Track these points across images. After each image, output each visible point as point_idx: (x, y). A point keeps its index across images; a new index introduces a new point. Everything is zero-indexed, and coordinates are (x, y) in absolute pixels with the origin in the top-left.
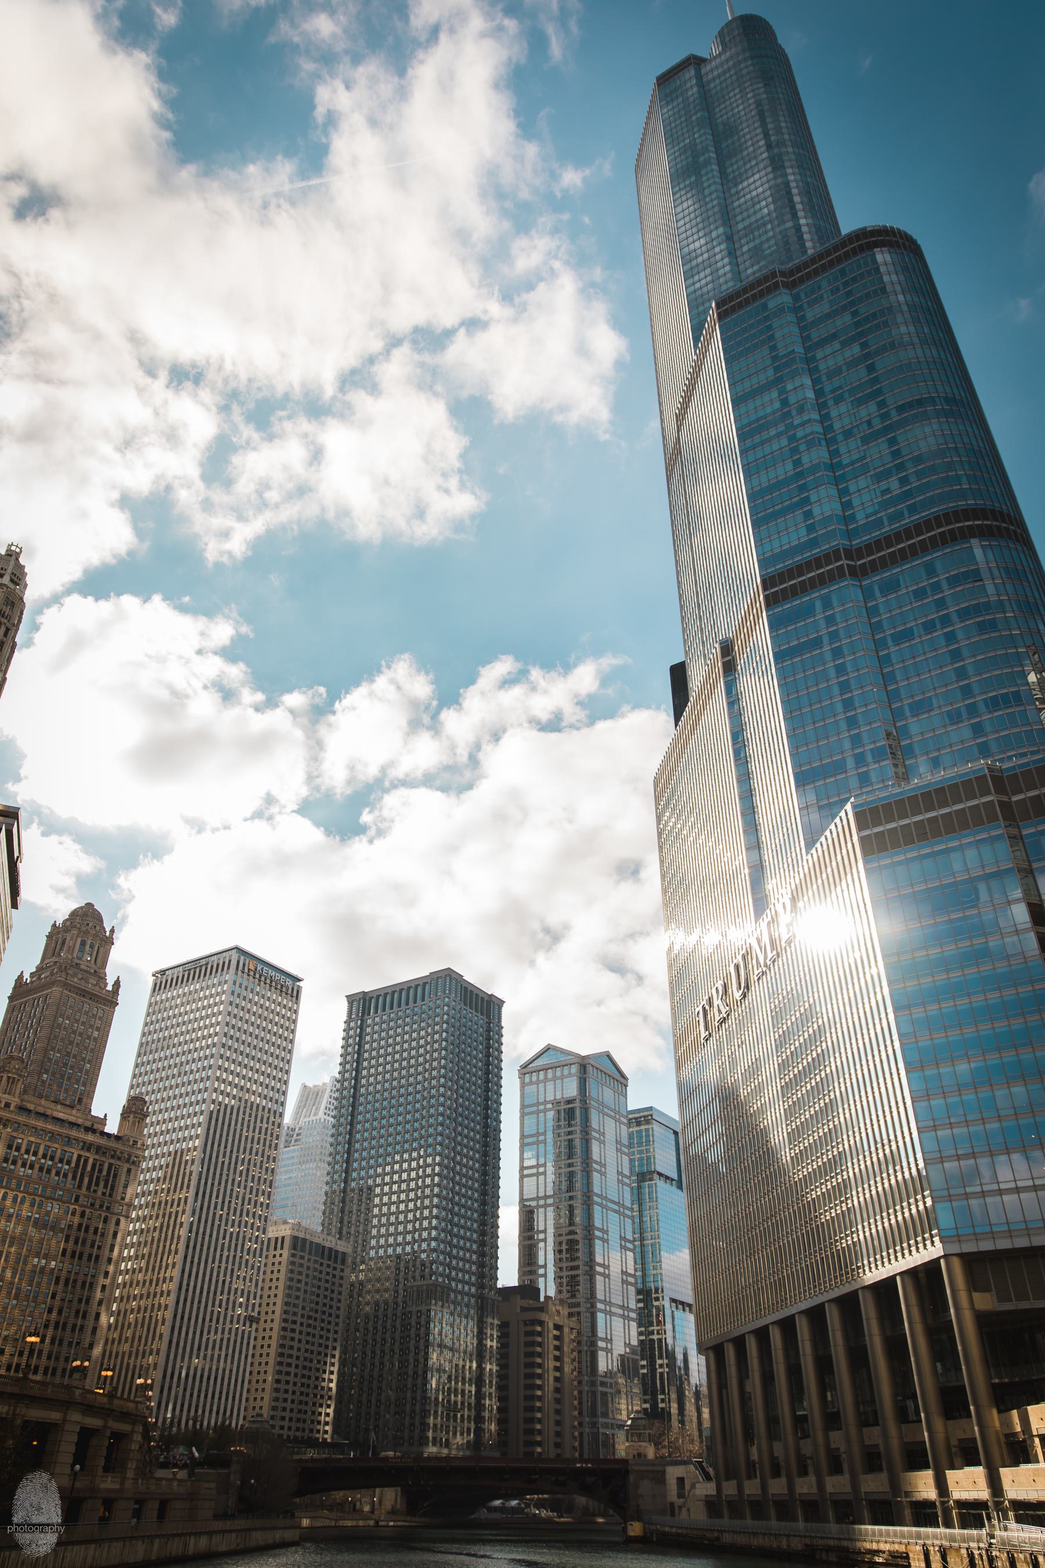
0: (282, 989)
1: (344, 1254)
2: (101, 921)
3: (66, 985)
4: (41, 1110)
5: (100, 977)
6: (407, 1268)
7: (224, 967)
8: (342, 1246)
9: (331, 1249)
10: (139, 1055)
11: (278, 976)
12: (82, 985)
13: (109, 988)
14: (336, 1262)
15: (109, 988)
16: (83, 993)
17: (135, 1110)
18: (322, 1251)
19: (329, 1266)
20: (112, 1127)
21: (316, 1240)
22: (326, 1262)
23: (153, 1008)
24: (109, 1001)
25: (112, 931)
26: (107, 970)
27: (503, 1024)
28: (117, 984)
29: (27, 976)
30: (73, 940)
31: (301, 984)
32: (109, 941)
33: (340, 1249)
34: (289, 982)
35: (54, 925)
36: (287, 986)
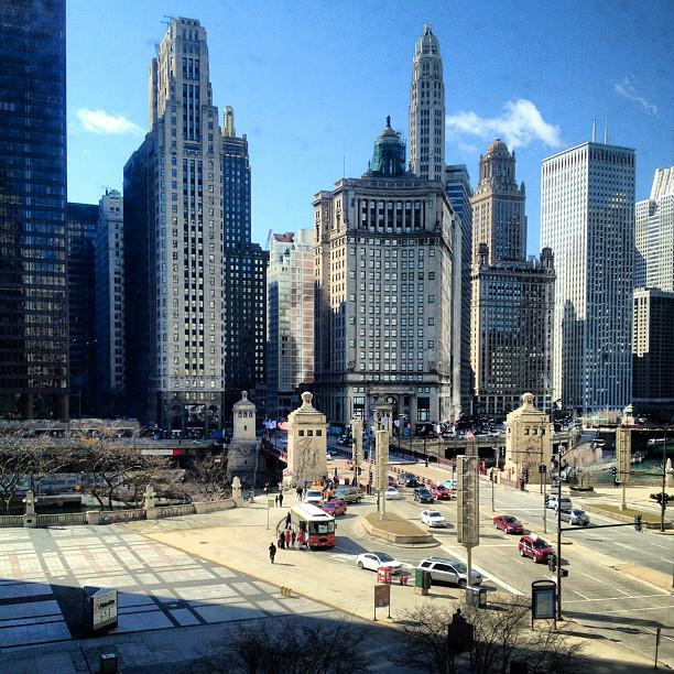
13: (519, 189)
26: (516, 179)
28: (523, 185)
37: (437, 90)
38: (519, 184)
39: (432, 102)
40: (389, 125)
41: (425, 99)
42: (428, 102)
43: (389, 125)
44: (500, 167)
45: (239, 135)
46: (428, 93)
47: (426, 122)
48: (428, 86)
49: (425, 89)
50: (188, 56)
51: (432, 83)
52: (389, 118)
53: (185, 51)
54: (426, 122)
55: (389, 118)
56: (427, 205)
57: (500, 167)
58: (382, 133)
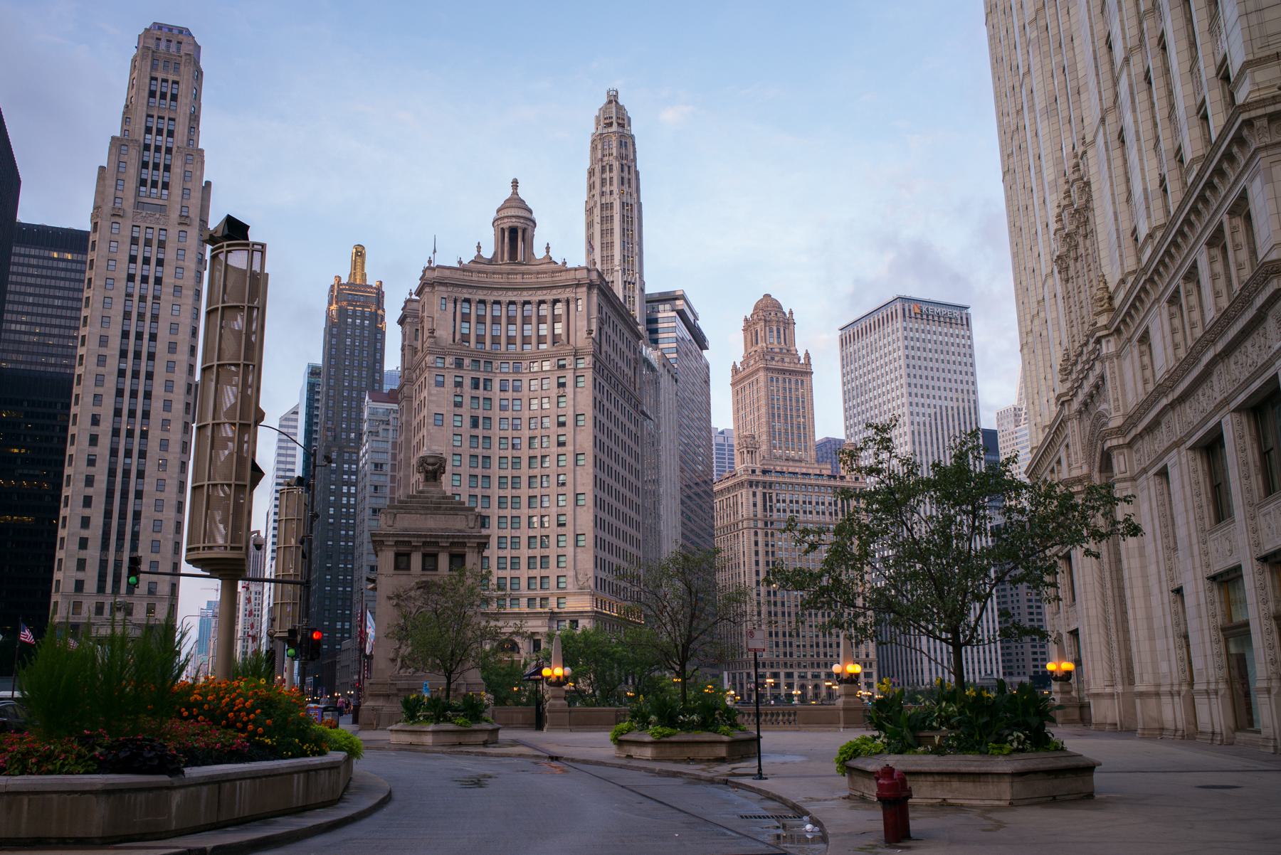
0: (951, 321)
2: (780, 307)
3: (767, 369)
4: (778, 469)
7: (891, 317)
10: (845, 402)
11: (944, 310)
15: (802, 361)
16: (784, 371)
23: (846, 361)
24: (803, 373)
25: (791, 313)
28: (807, 355)
29: (739, 365)
31: (969, 311)
34: (956, 313)
35: (746, 320)
36: (955, 317)
37: (626, 174)
38: (801, 354)
39: (616, 191)
40: (515, 193)
41: (607, 189)
42: (611, 192)
43: (515, 193)
44: (771, 331)
45: (372, 281)
46: (611, 178)
47: (606, 219)
48: (611, 170)
49: (607, 175)
50: (160, 75)
51: (616, 165)
52: (515, 184)
53: (154, 67)
54: (606, 219)
55: (515, 184)
56: (572, 306)
57: (771, 331)
58: (500, 203)
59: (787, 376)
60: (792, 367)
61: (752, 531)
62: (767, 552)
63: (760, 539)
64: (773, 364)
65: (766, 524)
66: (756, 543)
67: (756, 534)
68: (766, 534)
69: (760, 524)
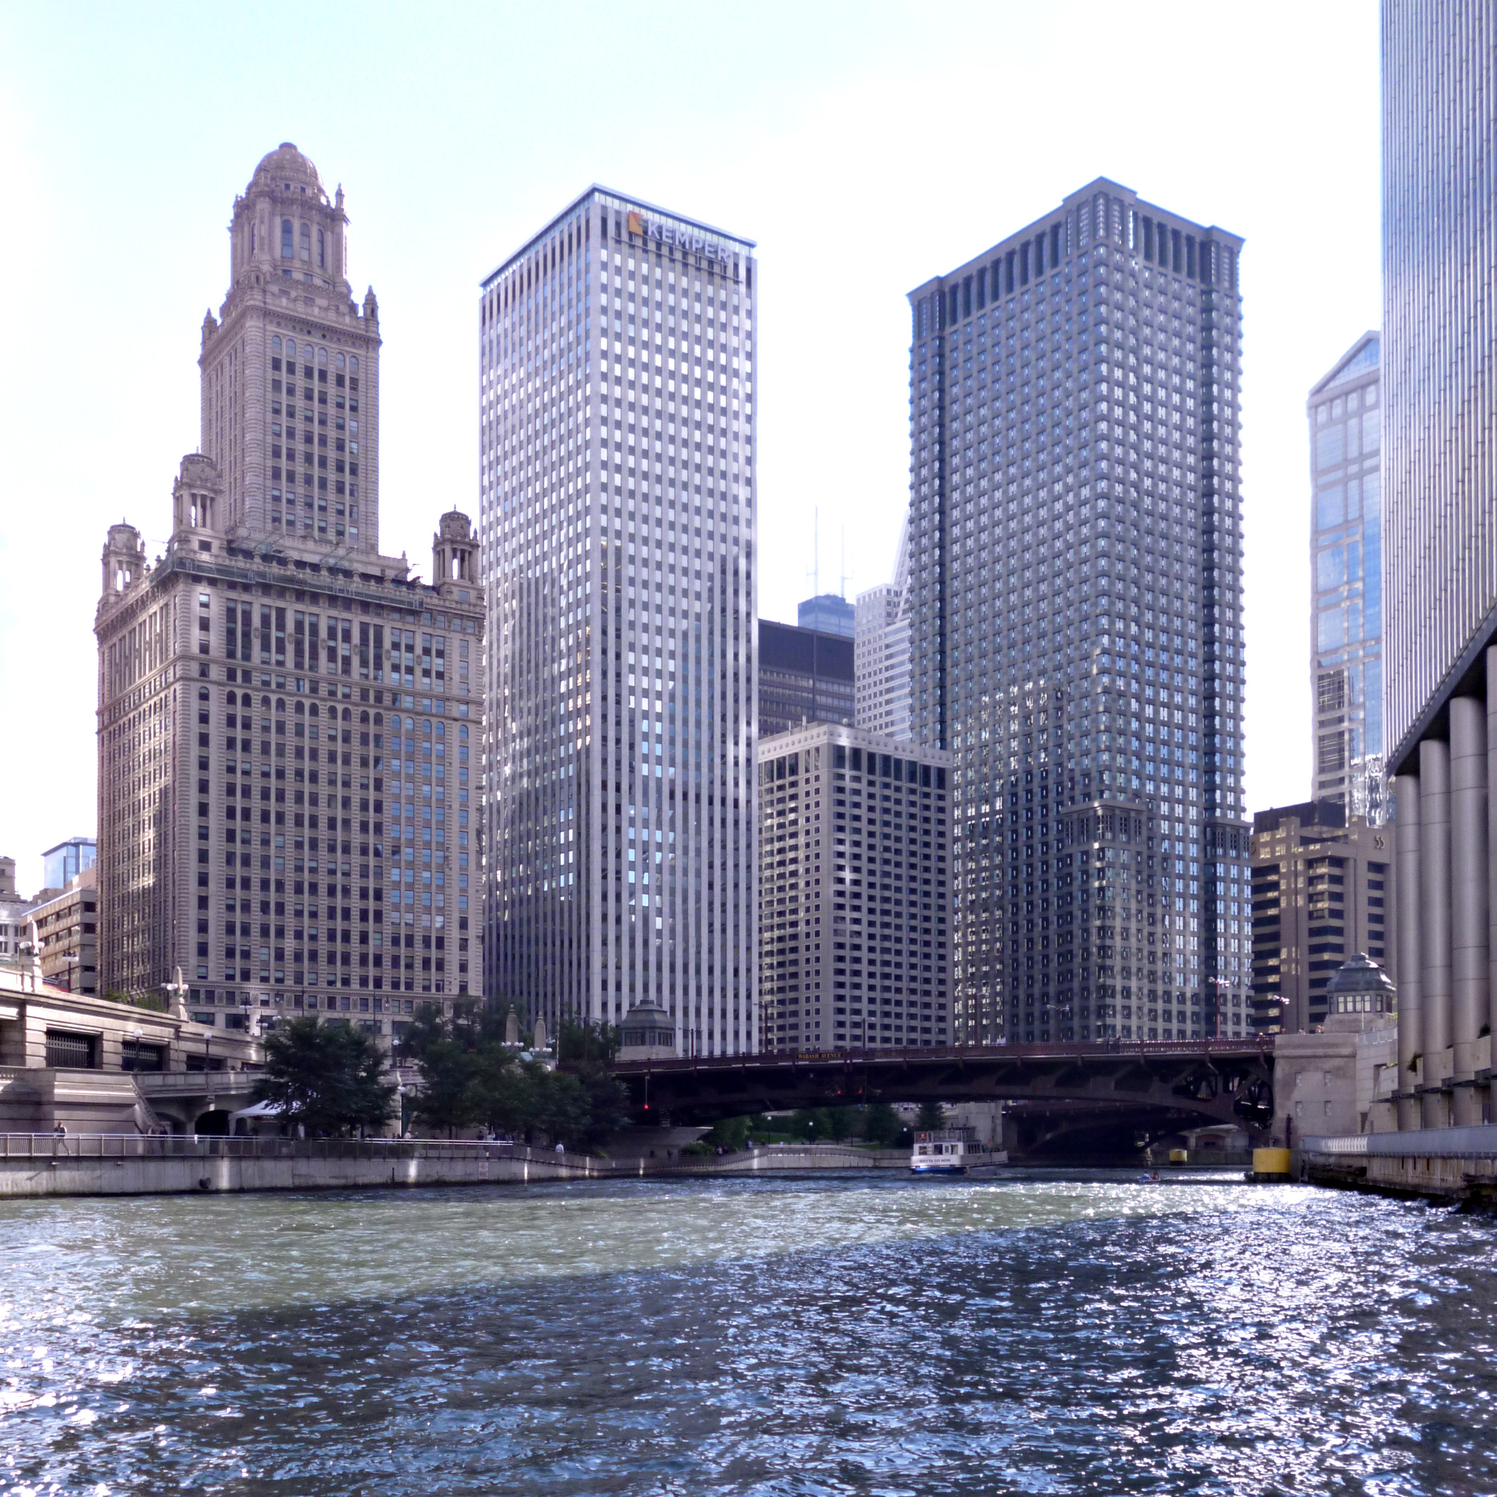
1: (941, 773)
5: (339, 292)
6: (1059, 784)
8: (932, 757)
9: (913, 764)
12: (300, 310)
14: (926, 783)
17: (454, 538)
18: (890, 765)
19: (913, 791)
20: (423, 570)
21: (905, 756)
22: (905, 784)
25: (339, 195)
27: (1247, 284)
30: (268, 225)
32: (334, 218)
33: (934, 763)
38: (358, 298)
44: (287, 229)
59: (316, 339)
60: (331, 319)
61: (195, 687)
62: (231, 743)
63: (216, 708)
64: (282, 305)
65: (231, 675)
66: (204, 719)
67: (204, 697)
68: (231, 698)
69: (216, 673)
